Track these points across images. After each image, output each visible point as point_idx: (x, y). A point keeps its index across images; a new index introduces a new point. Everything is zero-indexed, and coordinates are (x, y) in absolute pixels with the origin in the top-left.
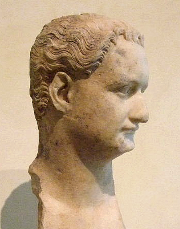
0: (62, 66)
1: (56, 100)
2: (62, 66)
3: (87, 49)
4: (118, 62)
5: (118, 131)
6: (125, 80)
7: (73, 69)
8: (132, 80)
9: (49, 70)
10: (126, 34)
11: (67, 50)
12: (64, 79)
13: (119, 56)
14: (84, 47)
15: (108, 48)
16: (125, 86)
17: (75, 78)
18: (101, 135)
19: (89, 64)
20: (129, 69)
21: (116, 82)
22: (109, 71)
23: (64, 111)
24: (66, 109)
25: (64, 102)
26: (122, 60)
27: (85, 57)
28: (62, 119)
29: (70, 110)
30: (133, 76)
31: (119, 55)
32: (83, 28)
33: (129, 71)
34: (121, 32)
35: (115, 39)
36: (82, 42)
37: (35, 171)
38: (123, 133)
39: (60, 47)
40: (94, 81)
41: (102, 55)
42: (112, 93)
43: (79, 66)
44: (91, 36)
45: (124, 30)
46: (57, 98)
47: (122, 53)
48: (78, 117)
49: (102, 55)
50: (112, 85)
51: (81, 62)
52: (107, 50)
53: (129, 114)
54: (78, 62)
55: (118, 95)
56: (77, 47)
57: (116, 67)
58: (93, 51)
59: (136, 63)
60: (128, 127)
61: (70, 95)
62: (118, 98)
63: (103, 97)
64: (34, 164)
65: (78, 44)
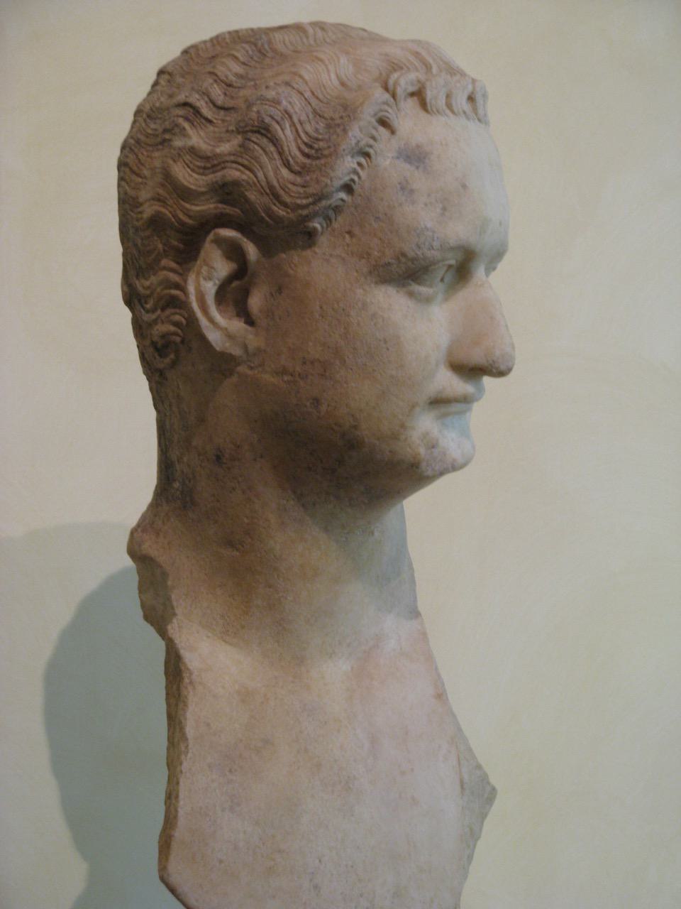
0: (228, 210)
1: (211, 320)
2: (228, 210)
3: (307, 156)
4: (405, 187)
5: (417, 409)
6: (431, 248)
7: (262, 220)
8: (452, 242)
9: (183, 224)
10: (429, 95)
11: (240, 160)
12: (234, 252)
13: (405, 168)
14: (292, 147)
15: (371, 146)
17: (266, 247)
19: (314, 203)
20: (444, 209)
21: (404, 255)
22: (377, 218)
23: (237, 352)
24: (245, 347)
25: (237, 325)
26: (420, 182)
27: (299, 180)
28: (234, 379)
29: (259, 351)
30: (458, 231)
31: (407, 166)
32: (287, 84)
34: (411, 89)
35: (391, 114)
36: (286, 135)
37: (150, 547)
39: (218, 151)
40: (331, 255)
41: (355, 172)
43: (281, 212)
44: (315, 112)
46: (214, 311)
47: (416, 156)
48: (284, 371)
49: (355, 172)
50: (389, 264)
51: (288, 200)
52: (367, 155)
54: (277, 197)
55: (411, 295)
56: (272, 149)
58: (323, 161)
60: (449, 393)
61: (256, 302)
63: (365, 306)
64: (147, 525)
65: (275, 141)
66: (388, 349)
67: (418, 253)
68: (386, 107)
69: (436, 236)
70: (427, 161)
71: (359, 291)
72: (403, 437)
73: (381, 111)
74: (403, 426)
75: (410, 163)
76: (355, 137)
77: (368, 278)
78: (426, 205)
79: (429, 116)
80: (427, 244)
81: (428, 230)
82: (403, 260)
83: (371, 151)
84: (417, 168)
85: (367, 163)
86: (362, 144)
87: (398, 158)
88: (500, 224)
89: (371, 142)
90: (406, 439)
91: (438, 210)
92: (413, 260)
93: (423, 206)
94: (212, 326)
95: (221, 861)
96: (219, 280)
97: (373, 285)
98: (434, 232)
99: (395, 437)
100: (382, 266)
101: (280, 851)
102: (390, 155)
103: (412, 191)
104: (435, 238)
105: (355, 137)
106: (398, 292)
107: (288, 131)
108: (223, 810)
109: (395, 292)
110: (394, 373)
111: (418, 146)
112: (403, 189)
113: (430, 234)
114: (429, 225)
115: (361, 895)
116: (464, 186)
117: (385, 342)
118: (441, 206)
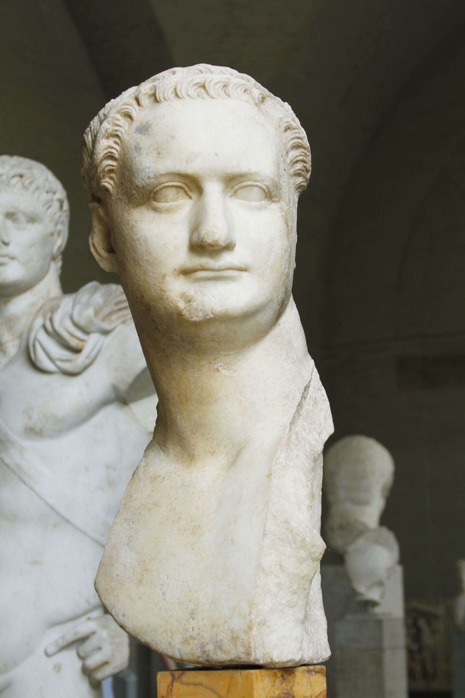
6: (149, 178)
15: (117, 131)
20: (159, 153)
31: (139, 135)
52: (117, 136)
68: (126, 106)
69: (151, 170)
70: (150, 129)
72: (165, 298)
74: (162, 290)
76: (104, 128)
77: (129, 205)
78: (147, 154)
83: (118, 133)
86: (110, 131)
88: (216, 154)
89: (117, 128)
90: (168, 298)
95: (118, 576)
101: (146, 570)
104: (150, 172)
106: (148, 210)
108: (124, 545)
109: (146, 210)
111: (147, 122)
113: (148, 170)
115: (190, 601)
116: (173, 137)
118: (156, 152)
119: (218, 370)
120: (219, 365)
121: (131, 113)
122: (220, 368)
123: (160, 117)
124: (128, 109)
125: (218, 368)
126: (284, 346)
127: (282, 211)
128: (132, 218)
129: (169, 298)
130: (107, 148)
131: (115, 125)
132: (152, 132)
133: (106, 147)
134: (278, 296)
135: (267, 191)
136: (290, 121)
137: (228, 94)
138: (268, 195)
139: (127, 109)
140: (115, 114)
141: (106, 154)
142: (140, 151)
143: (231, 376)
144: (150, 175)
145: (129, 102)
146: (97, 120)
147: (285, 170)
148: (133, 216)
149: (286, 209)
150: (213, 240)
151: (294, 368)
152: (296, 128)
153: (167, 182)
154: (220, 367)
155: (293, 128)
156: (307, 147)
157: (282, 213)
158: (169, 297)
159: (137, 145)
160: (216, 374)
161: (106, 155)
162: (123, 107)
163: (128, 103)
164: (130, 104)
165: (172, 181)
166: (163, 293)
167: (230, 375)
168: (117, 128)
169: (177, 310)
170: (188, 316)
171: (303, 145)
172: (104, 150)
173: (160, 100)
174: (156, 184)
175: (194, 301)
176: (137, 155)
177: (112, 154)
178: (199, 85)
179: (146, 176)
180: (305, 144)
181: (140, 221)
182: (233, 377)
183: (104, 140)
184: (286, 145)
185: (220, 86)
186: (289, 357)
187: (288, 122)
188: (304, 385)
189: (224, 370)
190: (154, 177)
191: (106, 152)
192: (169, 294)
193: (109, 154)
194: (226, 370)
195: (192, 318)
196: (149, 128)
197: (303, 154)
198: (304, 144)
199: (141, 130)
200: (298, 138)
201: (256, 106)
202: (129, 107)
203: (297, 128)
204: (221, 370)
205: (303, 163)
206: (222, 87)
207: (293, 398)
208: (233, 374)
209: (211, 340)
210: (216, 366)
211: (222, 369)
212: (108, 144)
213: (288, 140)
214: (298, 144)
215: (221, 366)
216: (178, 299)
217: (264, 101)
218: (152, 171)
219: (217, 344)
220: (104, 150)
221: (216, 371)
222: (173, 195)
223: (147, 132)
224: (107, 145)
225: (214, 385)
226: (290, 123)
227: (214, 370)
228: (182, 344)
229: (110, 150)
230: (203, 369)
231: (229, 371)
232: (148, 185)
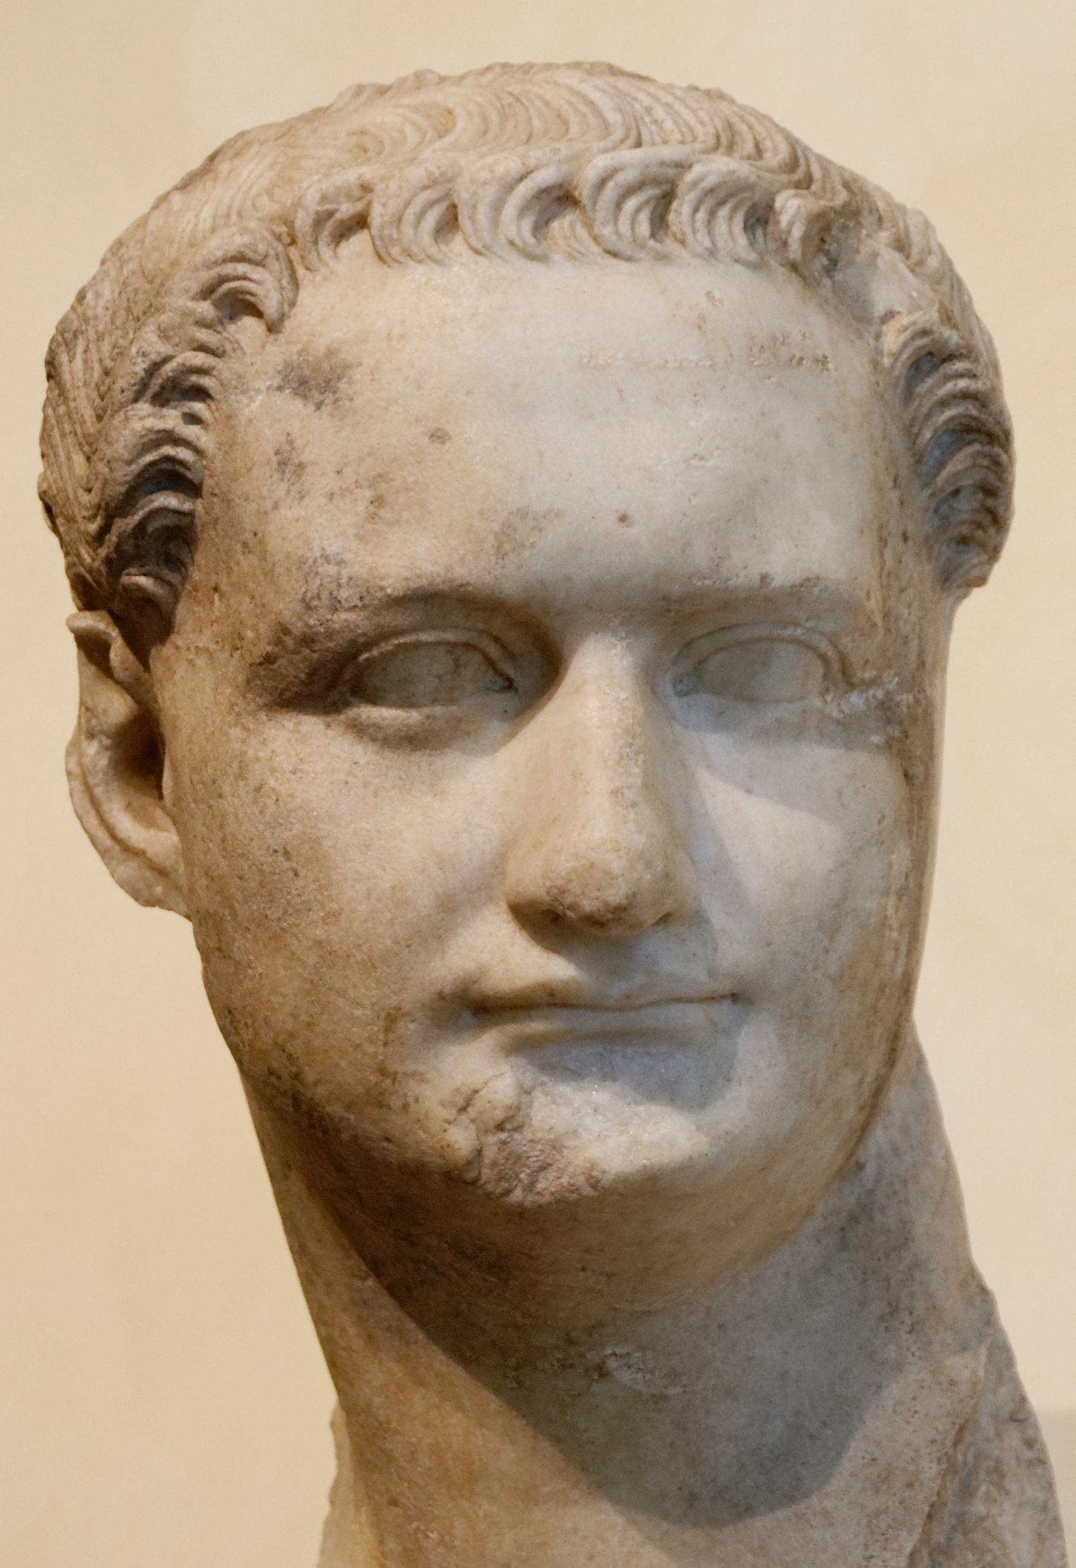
5: (408, 1029)
6: (335, 605)
16: (357, 647)
18: (310, 1076)
20: (378, 501)
31: (297, 405)
33: (372, 517)
38: (490, 1039)
42: (311, 724)
45: (366, 188)
52: (201, 394)
53: (498, 866)
55: (359, 730)
57: (276, 506)
59: (439, 436)
62: (363, 753)
66: (296, 874)
67: (312, 622)
68: (241, 268)
69: (345, 573)
70: (342, 385)
71: (235, 732)
72: (396, 1102)
73: (223, 280)
75: (305, 397)
76: (144, 355)
77: (249, 696)
79: (385, 268)
80: (324, 595)
81: (327, 558)
82: (289, 642)
83: (206, 382)
84: (319, 406)
85: (212, 412)
86: (168, 369)
87: (280, 388)
89: (200, 359)
90: (405, 1107)
91: (362, 506)
92: (308, 640)
93: (323, 501)
94: (117, 847)
96: (108, 737)
97: (263, 716)
98: (341, 563)
99: (378, 1100)
100: (261, 664)
102: (262, 385)
103: (301, 466)
104: (344, 581)
105: (144, 355)
106: (328, 726)
107: (78, 364)
109: (322, 726)
110: (319, 933)
111: (330, 353)
112: (283, 464)
114: (332, 549)
117: (286, 853)
118: (369, 494)
119: (602, 1371)
120: (609, 1351)
121: (263, 299)
122: (612, 1364)
123: (389, 337)
124: (250, 280)
125: (603, 1362)
126: (879, 1260)
127: (888, 721)
128: (261, 754)
129: (413, 1108)
130: (157, 444)
131: (195, 345)
132: (351, 400)
133: (153, 436)
134: (861, 1082)
135: (830, 653)
136: (935, 328)
137: (679, 236)
138: (836, 667)
139: (244, 278)
140: (193, 299)
141: (152, 464)
142: (299, 476)
143: (653, 1396)
144: (344, 594)
145: (255, 252)
146: (113, 292)
147: (905, 538)
148: (264, 743)
149: (905, 710)
150: (606, 903)
151: (917, 1354)
152: (957, 353)
153: (413, 629)
154: (613, 1358)
155: (948, 353)
156: (1000, 434)
157: (889, 729)
158: (411, 1100)
159: (288, 448)
160: (596, 1388)
161: (151, 471)
162: (229, 269)
163: (251, 255)
164: (259, 258)
165: (433, 628)
166: (388, 1082)
167: (652, 1391)
168: (200, 359)
169: (442, 1156)
170: (490, 1187)
171: (984, 424)
172: (145, 449)
173: (389, 254)
174: (364, 634)
175: (518, 1129)
176: (288, 492)
177: (182, 470)
178: (556, 193)
179: (323, 597)
180: (994, 418)
181: (294, 772)
182: (666, 1398)
183: (144, 407)
184: (915, 430)
185: (647, 202)
186: (897, 1306)
187: (925, 333)
188: (954, 1423)
189: (630, 1371)
190: (360, 604)
191: (149, 458)
192: (412, 1088)
193: (165, 466)
194: (637, 1373)
195: (507, 1192)
196: (339, 379)
197: (985, 462)
198: (991, 419)
199: (303, 382)
200: (966, 396)
201: (794, 275)
202: (256, 273)
203: (964, 351)
204: (614, 1373)
205: (980, 496)
206: (652, 203)
207: (910, 1485)
208: (666, 1388)
209: (579, 1266)
210: (593, 1357)
211: (621, 1367)
212: (160, 425)
213: (924, 410)
214: (965, 421)
215: (615, 1354)
216: (450, 1113)
217: (828, 240)
218: (351, 578)
219: (604, 1279)
220: (145, 449)
221: (596, 1377)
222: (440, 677)
223: (329, 398)
224: (159, 432)
225: (586, 1431)
226: (936, 335)
227: (587, 1370)
228: (458, 1266)
229: (168, 450)
230: (539, 1364)
231: (648, 1376)
232: (330, 634)
